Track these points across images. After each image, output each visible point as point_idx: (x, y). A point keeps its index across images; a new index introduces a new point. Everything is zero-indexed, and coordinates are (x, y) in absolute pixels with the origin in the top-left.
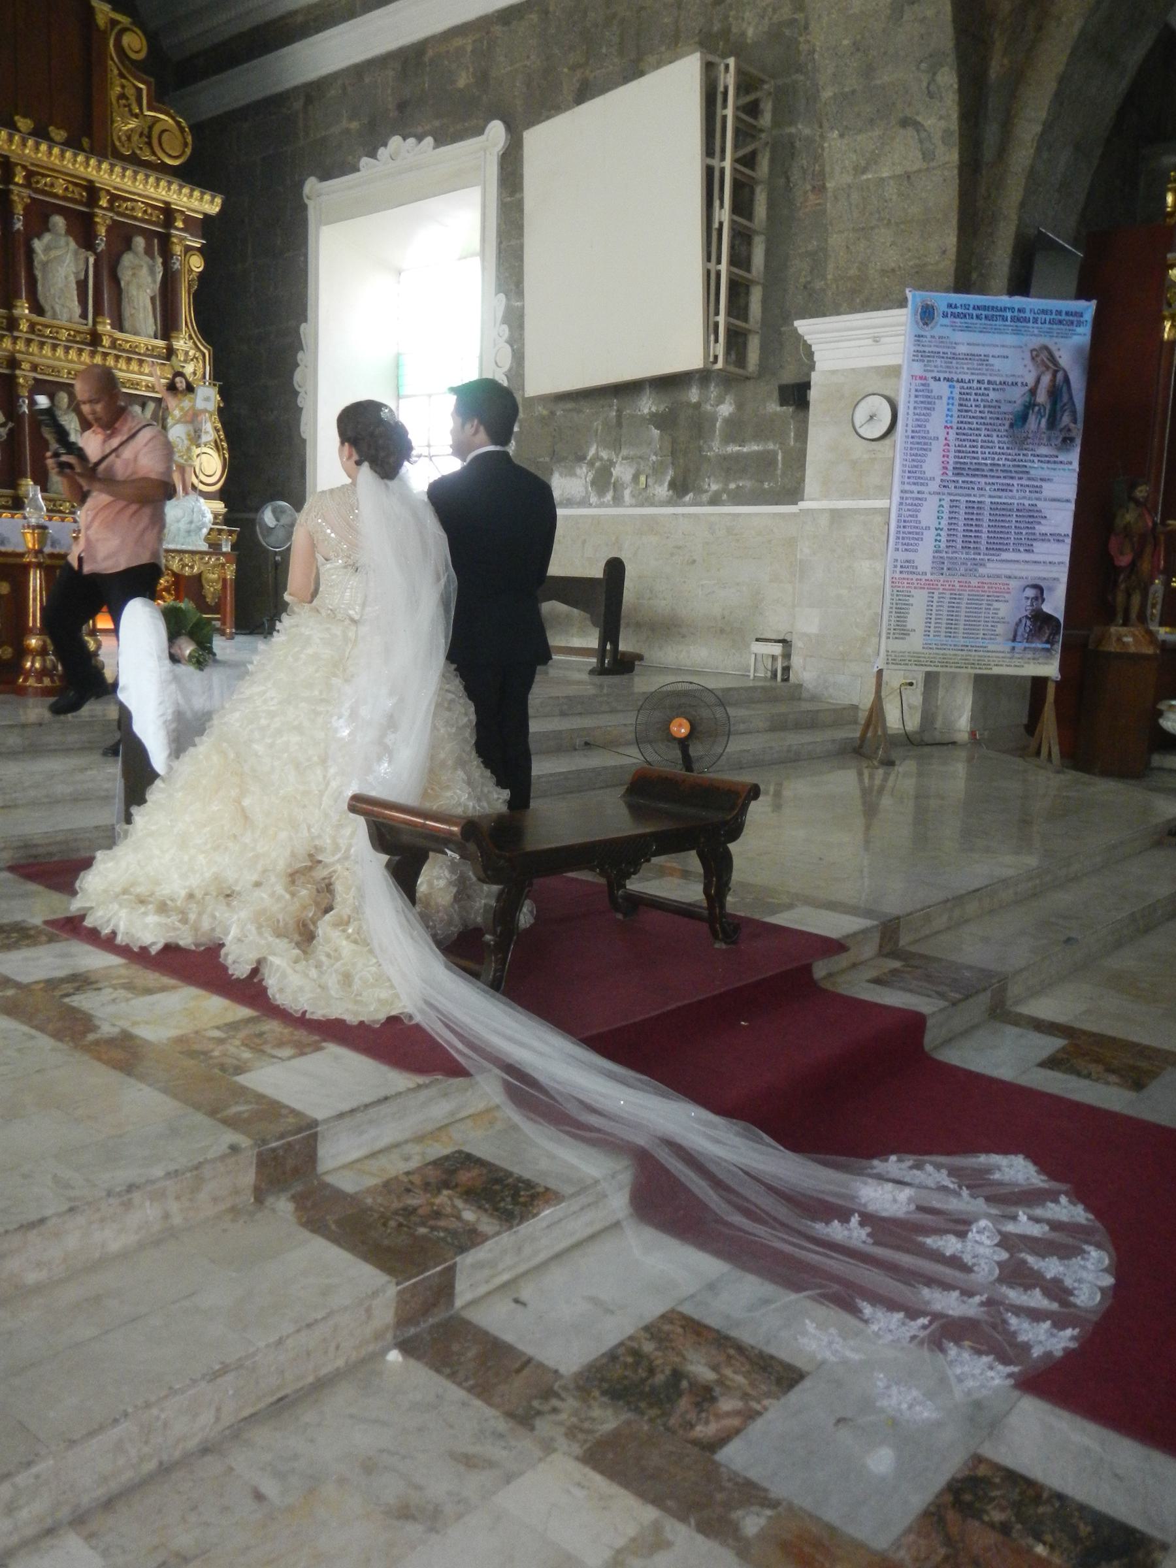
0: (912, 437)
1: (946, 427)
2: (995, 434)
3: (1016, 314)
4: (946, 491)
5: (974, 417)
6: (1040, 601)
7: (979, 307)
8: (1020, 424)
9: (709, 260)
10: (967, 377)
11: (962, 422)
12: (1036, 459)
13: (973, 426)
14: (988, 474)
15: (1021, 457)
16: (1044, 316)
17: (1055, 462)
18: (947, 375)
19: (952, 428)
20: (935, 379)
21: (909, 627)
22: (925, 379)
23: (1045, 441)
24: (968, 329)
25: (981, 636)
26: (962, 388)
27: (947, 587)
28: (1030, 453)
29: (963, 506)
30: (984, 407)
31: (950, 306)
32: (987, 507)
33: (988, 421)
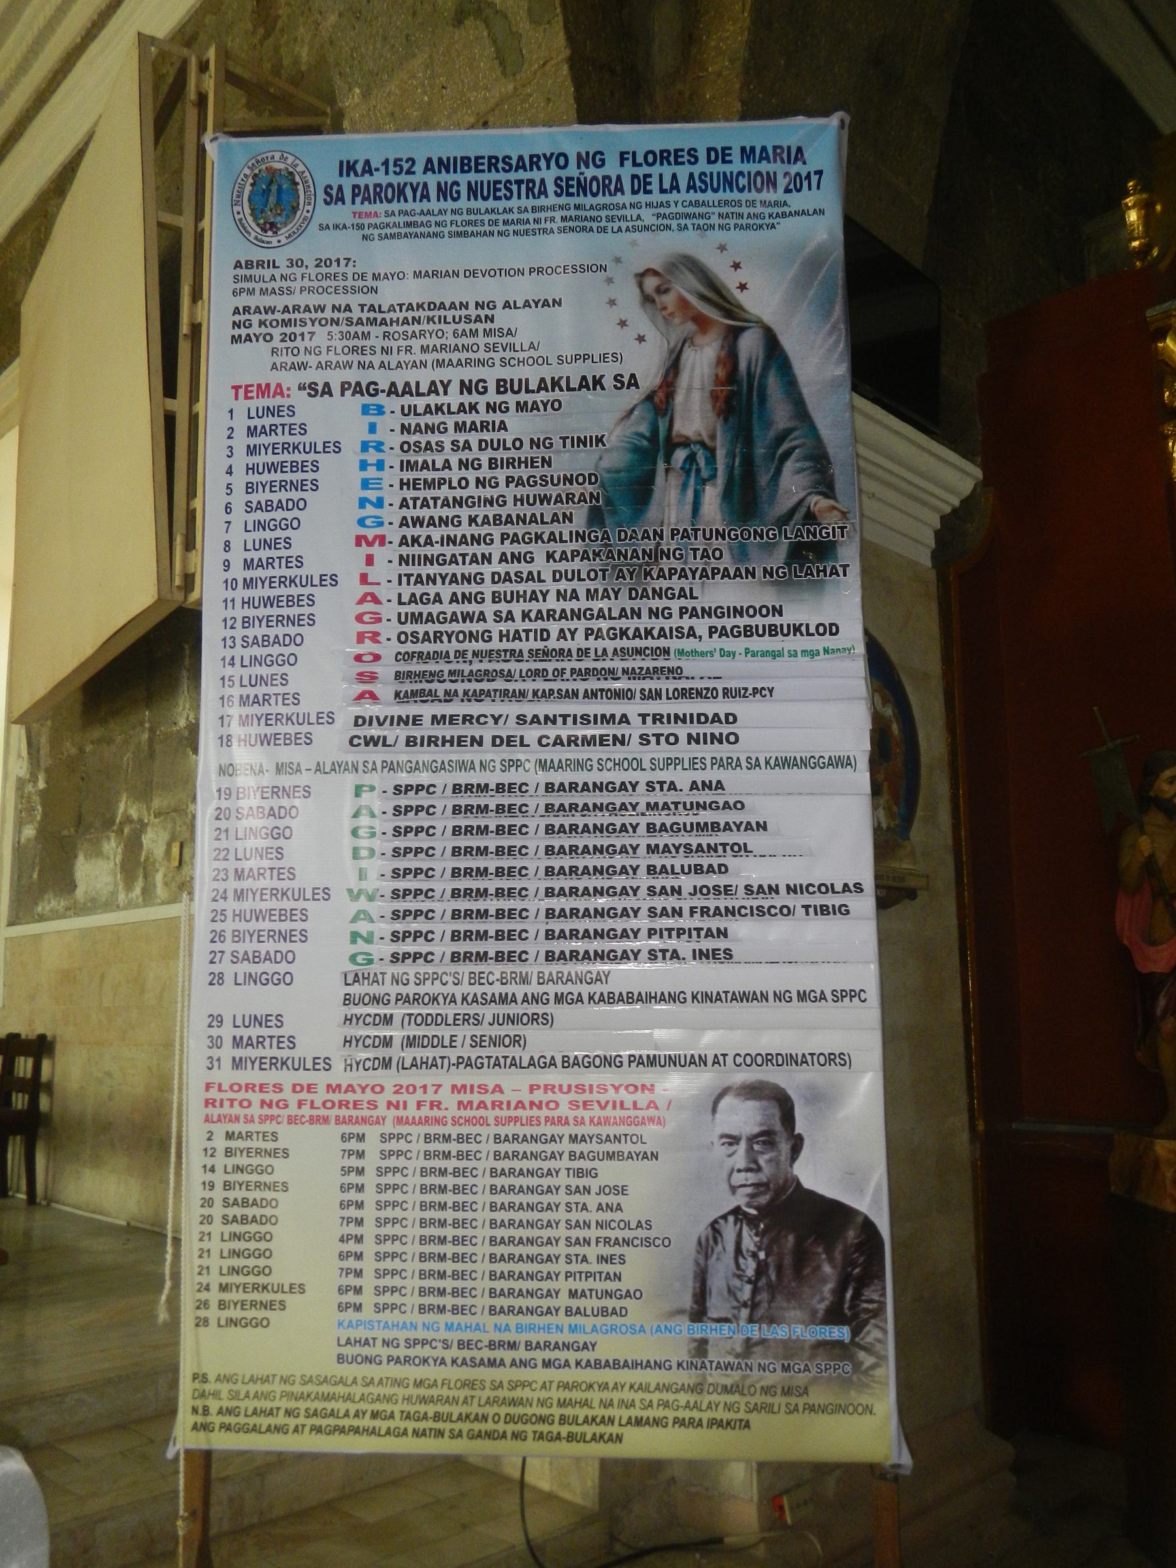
0: (248, 584)
1: (359, 540)
2: (539, 551)
3: (572, 171)
4: (377, 755)
5: (458, 502)
6: (785, 1147)
7: (444, 165)
8: (625, 510)
9: (170, 390)
10: (424, 377)
11: (418, 522)
12: (702, 626)
13: (458, 532)
14: (529, 686)
15: (645, 622)
16: (667, 171)
17: (773, 631)
18: (352, 376)
19: (382, 540)
20: (312, 389)
21: (282, 1274)
22: (279, 391)
23: (726, 562)
24: (412, 230)
25: (563, 1301)
26: (412, 410)
27: (412, 1112)
28: (675, 605)
29: (444, 802)
30: (493, 465)
31: (348, 168)
32: (536, 801)
33: (510, 509)
